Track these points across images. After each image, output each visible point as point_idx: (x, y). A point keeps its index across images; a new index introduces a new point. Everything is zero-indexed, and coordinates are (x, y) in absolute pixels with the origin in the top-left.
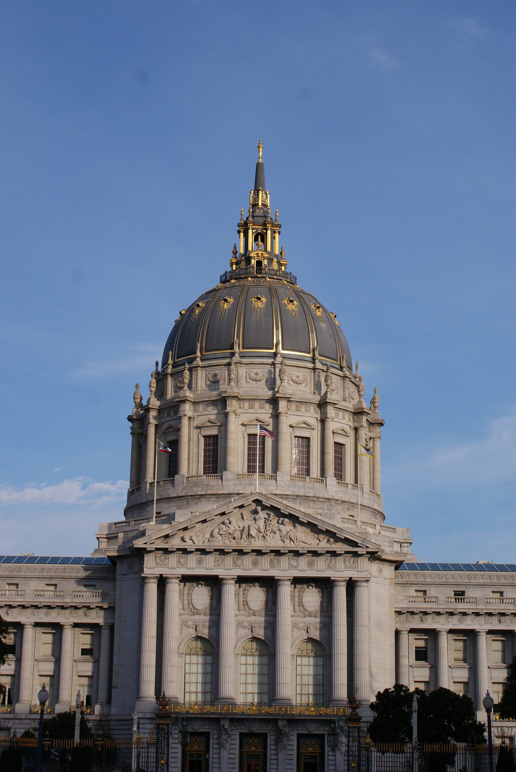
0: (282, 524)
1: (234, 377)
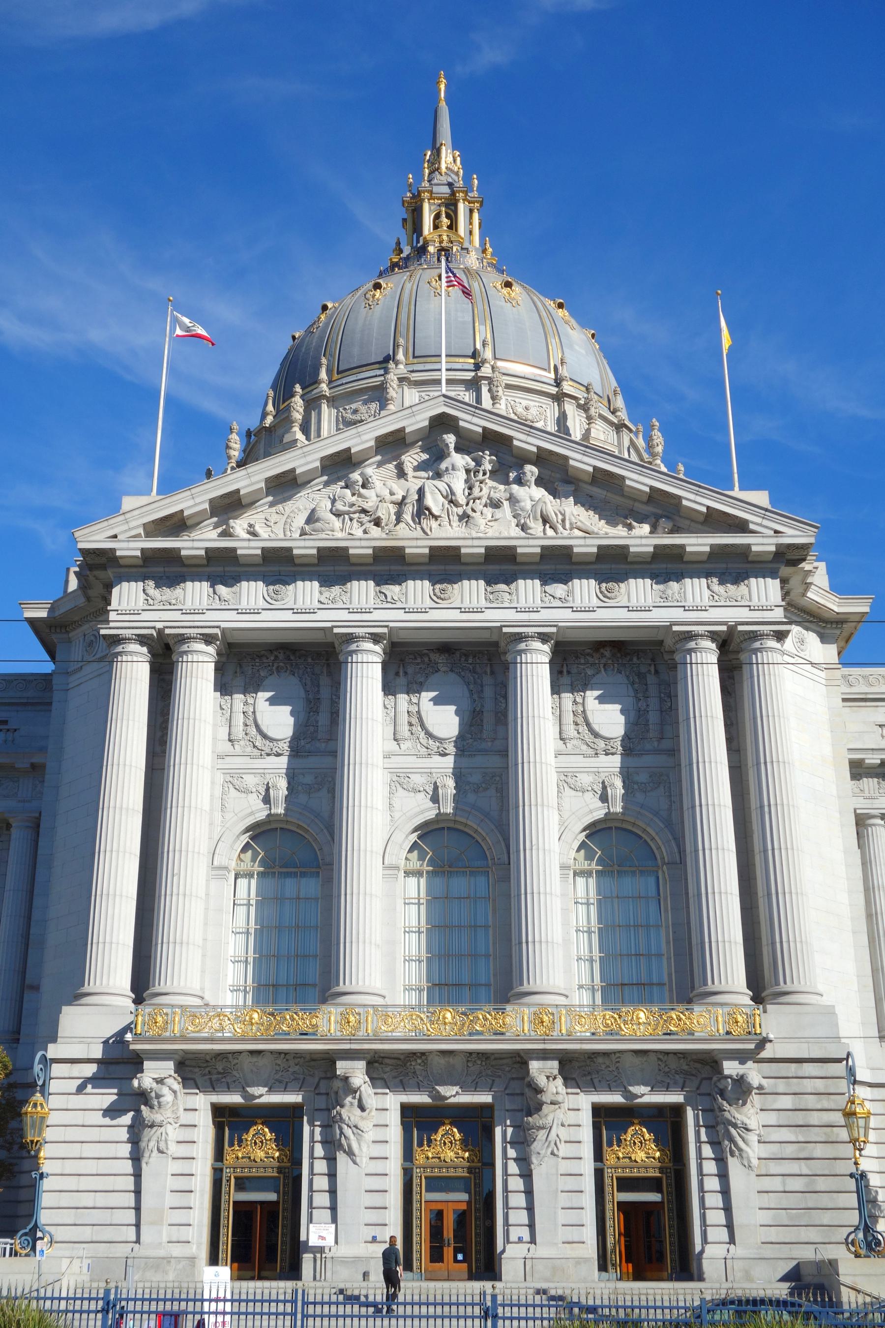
0: (520, 481)
1: (394, 395)
